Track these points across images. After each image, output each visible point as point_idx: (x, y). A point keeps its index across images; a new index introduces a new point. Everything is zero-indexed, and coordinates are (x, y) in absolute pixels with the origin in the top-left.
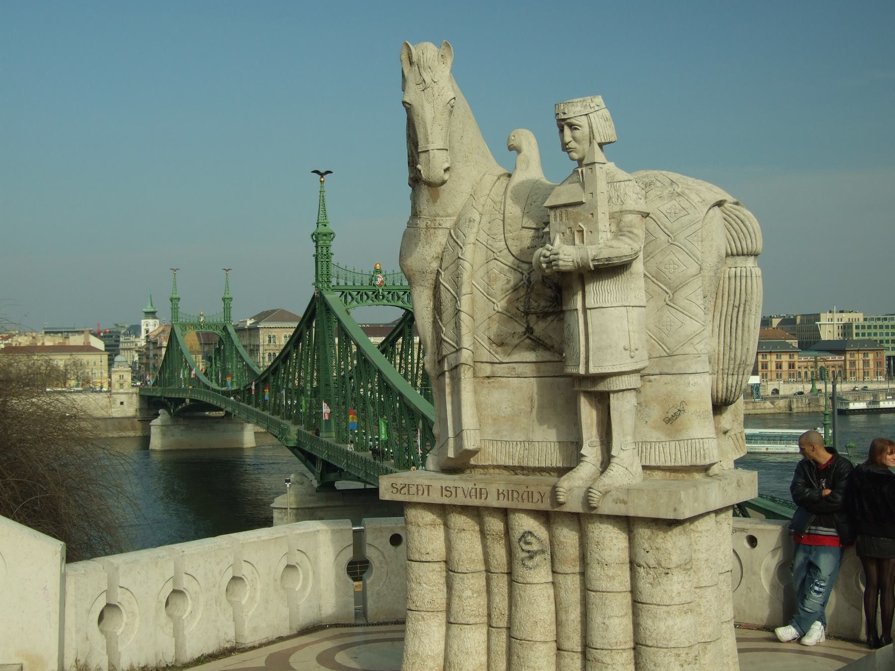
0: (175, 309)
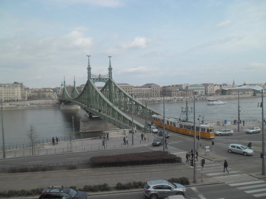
0: (65, 84)
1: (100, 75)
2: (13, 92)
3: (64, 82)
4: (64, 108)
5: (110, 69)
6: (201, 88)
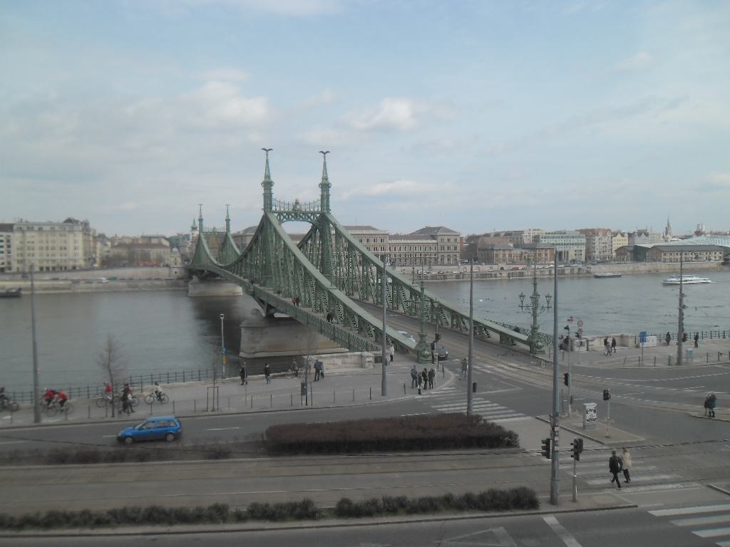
0: (201, 225)
1: (297, 203)
2: (63, 245)
3: (201, 220)
5: (325, 186)
6: (575, 241)
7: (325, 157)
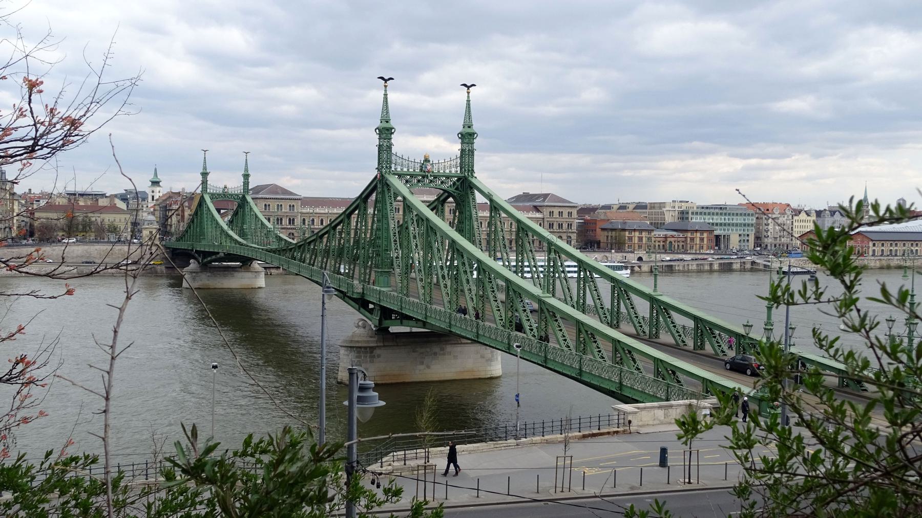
1: (427, 160)
4: (195, 285)
6: (740, 220)
7: (468, 93)
